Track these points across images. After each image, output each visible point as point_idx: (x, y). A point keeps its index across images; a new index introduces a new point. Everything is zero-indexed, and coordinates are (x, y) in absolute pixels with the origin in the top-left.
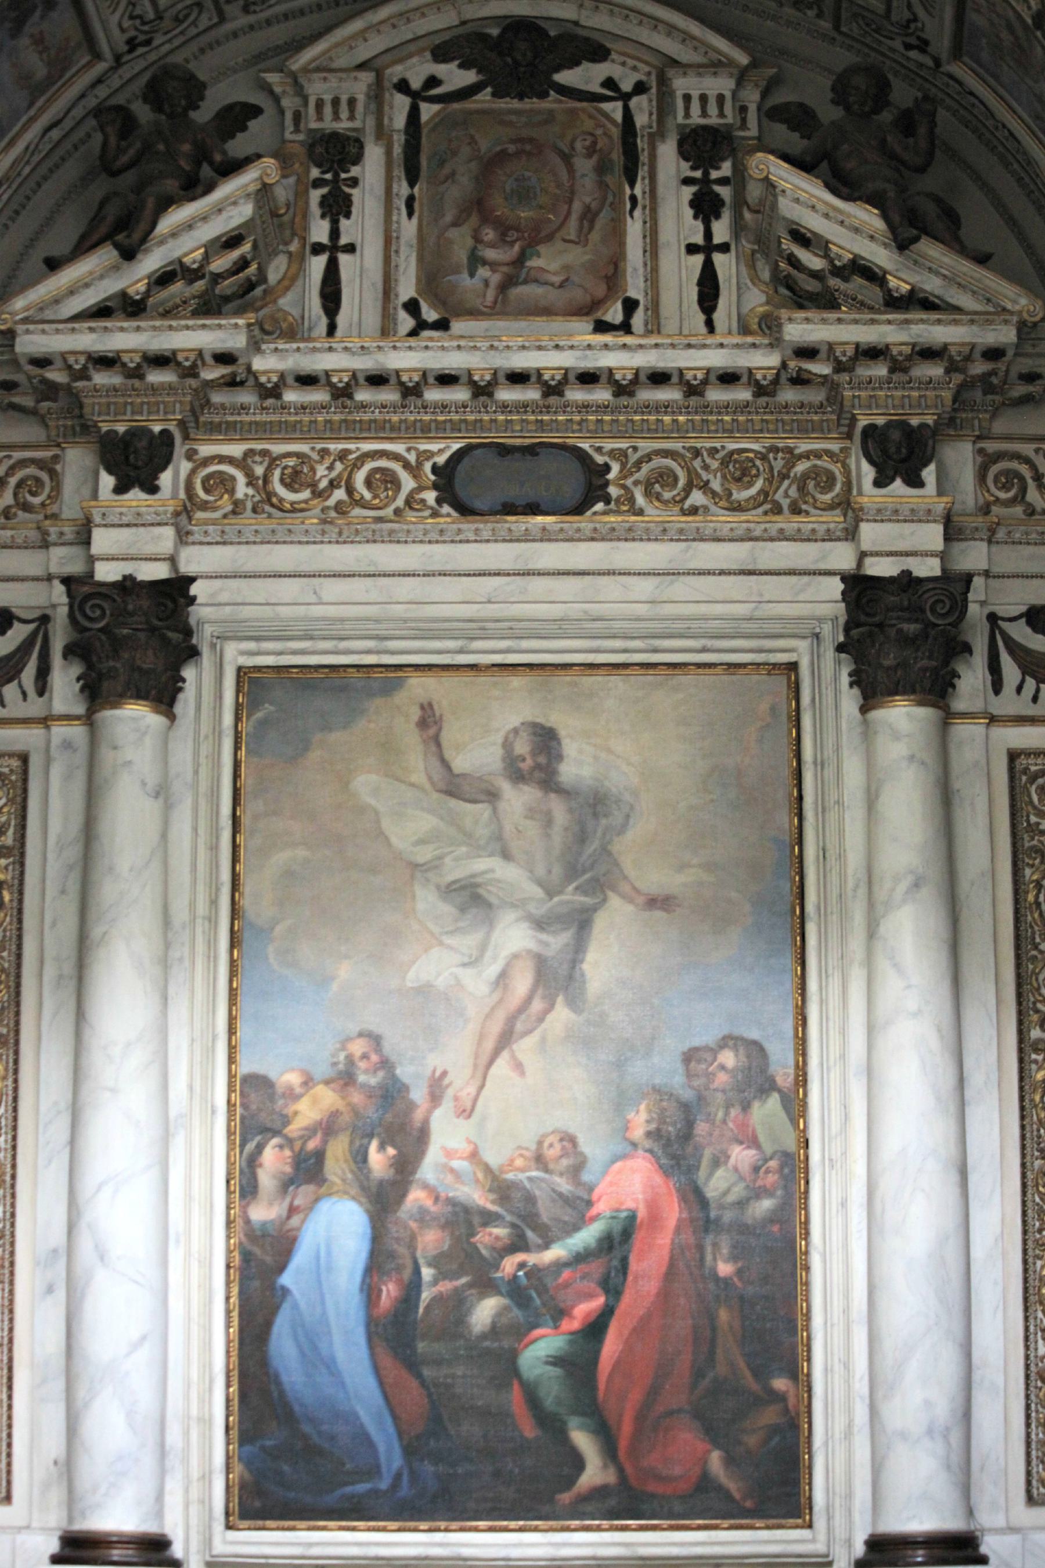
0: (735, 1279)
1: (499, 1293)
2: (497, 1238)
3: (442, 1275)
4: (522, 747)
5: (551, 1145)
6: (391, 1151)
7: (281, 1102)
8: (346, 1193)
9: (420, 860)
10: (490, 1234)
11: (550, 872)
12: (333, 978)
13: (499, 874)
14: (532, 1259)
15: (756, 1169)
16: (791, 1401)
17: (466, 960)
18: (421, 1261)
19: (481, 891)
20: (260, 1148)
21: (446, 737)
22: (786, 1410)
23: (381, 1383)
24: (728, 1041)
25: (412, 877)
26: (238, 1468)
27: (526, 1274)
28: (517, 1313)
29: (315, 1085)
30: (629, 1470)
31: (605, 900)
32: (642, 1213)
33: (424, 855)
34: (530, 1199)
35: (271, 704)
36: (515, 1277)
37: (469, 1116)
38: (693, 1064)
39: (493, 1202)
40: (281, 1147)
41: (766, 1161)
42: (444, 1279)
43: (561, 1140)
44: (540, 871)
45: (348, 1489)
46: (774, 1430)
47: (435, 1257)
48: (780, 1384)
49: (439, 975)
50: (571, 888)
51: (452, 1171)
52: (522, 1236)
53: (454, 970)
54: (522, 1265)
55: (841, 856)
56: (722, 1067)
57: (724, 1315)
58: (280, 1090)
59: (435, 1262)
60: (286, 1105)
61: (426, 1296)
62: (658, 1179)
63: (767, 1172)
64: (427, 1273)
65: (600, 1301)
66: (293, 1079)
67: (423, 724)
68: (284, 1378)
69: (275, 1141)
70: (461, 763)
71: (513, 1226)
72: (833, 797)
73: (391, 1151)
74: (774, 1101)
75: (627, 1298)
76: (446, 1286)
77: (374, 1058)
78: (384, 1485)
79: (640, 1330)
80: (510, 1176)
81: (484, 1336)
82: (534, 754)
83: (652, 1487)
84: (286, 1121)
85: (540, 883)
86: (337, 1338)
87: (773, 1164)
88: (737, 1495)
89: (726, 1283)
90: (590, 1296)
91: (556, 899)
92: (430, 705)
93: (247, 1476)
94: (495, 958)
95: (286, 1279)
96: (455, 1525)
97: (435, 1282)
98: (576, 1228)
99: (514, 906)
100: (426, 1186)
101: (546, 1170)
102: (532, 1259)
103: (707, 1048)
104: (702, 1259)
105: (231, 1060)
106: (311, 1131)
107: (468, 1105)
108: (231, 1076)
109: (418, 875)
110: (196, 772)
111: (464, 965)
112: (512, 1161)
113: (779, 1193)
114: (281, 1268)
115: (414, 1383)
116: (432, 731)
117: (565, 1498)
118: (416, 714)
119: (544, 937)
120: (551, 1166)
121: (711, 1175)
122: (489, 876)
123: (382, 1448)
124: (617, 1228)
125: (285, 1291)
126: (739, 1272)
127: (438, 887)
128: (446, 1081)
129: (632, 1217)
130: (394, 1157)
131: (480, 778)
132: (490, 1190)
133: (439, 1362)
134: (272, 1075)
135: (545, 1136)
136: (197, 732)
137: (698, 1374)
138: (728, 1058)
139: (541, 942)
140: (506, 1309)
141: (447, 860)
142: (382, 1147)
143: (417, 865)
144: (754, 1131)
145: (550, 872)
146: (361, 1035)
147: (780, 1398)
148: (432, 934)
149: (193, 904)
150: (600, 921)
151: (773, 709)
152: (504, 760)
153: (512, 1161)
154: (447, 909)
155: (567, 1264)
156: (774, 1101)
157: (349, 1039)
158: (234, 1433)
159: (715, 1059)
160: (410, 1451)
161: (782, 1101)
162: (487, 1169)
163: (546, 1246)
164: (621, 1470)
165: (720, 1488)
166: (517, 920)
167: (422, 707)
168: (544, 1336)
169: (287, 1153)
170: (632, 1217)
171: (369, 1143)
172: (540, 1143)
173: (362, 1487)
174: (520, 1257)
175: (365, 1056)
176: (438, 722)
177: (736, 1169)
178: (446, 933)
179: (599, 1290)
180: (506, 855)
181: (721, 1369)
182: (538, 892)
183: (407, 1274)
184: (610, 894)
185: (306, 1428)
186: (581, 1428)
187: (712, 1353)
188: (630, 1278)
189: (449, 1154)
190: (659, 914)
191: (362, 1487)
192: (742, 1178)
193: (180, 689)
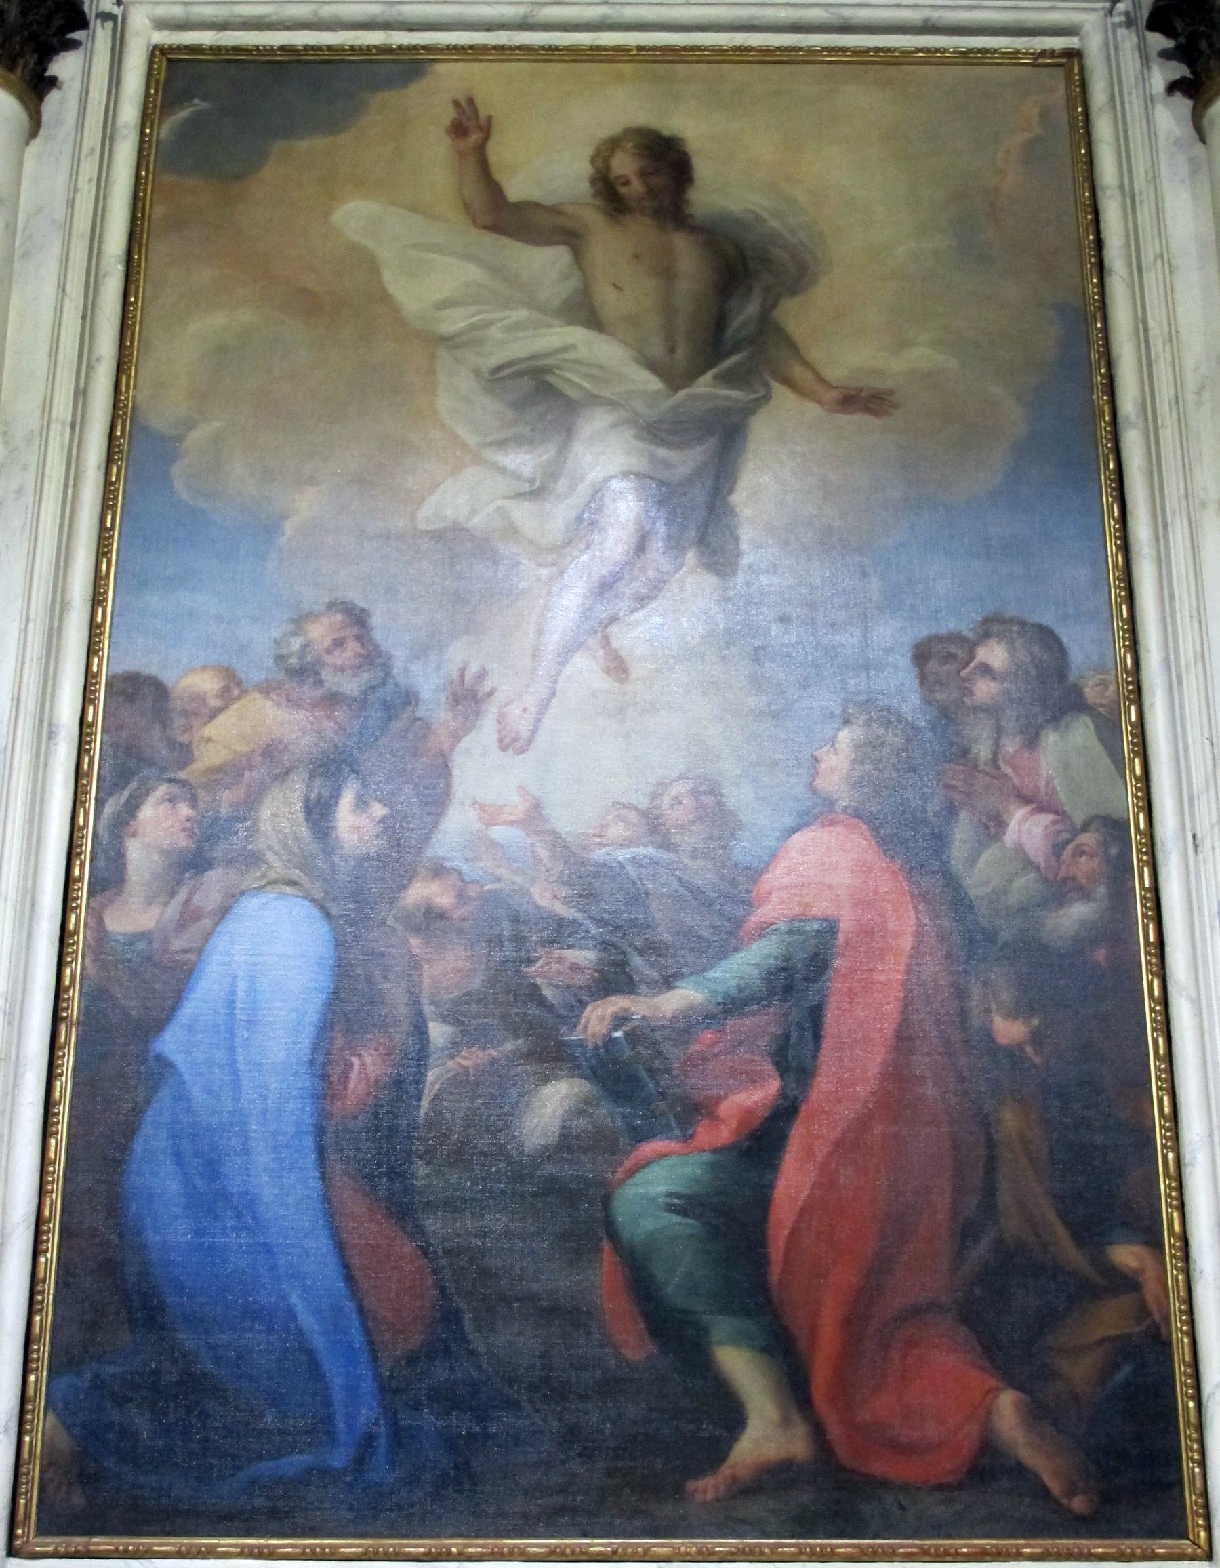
0: (1029, 1050)
1: (576, 1070)
2: (575, 967)
3: (467, 1037)
4: (624, 165)
5: (677, 801)
6: (379, 810)
7: (179, 722)
8: (292, 883)
9: (446, 328)
10: (560, 960)
11: (672, 350)
12: (284, 517)
13: (582, 353)
14: (640, 1007)
15: (1057, 849)
16: (1151, 1289)
17: (526, 487)
18: (428, 1009)
19: (550, 378)
20: (132, 808)
21: (497, 153)
22: (1143, 1310)
23: (340, 1247)
24: (991, 626)
25: (433, 357)
26: (41, 1422)
27: (627, 1034)
28: (608, 1114)
29: (244, 692)
30: (835, 1431)
31: (767, 397)
32: (846, 925)
33: (455, 322)
34: (637, 897)
35: (204, 98)
36: (610, 1042)
37: (522, 751)
38: (932, 665)
39: (566, 901)
40: (172, 800)
41: (1075, 833)
42: (470, 1045)
43: (695, 793)
44: (656, 348)
45: (264, 1468)
46: (1122, 1349)
47: (456, 1003)
48: (1126, 1255)
49: (474, 512)
50: (708, 377)
51: (493, 843)
52: (621, 965)
53: (499, 503)
54: (621, 1019)
55: (1172, 337)
56: (985, 669)
57: (1009, 1119)
58: (177, 704)
59: (452, 1016)
60: (188, 729)
61: (433, 1076)
62: (879, 861)
63: (1079, 852)
64: (438, 1032)
65: (773, 1086)
66: (207, 684)
67: (458, 130)
68: (152, 1238)
69: (162, 790)
70: (516, 189)
71: (605, 946)
72: (1149, 251)
73: (379, 810)
74: (1081, 732)
75: (823, 1084)
76: (472, 1059)
77: (352, 646)
78: (339, 1458)
79: (847, 1146)
80: (599, 855)
81: (546, 1154)
82: (643, 174)
83: (879, 1467)
84: (184, 754)
85: (653, 366)
86: (263, 1158)
87: (1088, 839)
88: (1054, 1486)
89: (1013, 1054)
90: (754, 1078)
91: (682, 393)
92: (471, 101)
93: (64, 1442)
94: (572, 489)
95: (170, 1043)
96: (476, 1546)
97: (454, 1046)
98: (724, 954)
99: (611, 404)
100: (438, 871)
101: (667, 846)
102: (640, 1007)
103: (955, 638)
104: (964, 1014)
105: (92, 649)
106: (229, 772)
107: (524, 733)
108: (90, 678)
109: (442, 353)
110: (71, 203)
111: (520, 495)
112: (604, 826)
113: (1102, 890)
114: (160, 1025)
115: (407, 1247)
116: (474, 138)
117: (707, 1487)
118: (450, 114)
119: (662, 452)
120: (676, 839)
121: (973, 859)
122: (567, 356)
123: (337, 1380)
124: (800, 956)
125: (165, 1064)
126: (1036, 1037)
127: (477, 373)
128: (487, 685)
129: (830, 929)
130: (383, 820)
131: (555, 210)
132: (561, 881)
133: (454, 1205)
134: (167, 677)
135: (663, 785)
136: (78, 144)
137: (967, 1233)
138: (995, 654)
139: (653, 458)
140: (587, 1101)
141: (495, 332)
142: (361, 803)
143: (444, 340)
144: (1049, 781)
145: (672, 350)
146: (331, 606)
147: (1128, 1283)
148: (465, 446)
149: (47, 405)
150: (761, 429)
151: (1044, 116)
152: (593, 181)
153: (604, 826)
154: (489, 408)
155: (709, 1017)
156: (1081, 732)
157: (311, 616)
158: (43, 1351)
159: (972, 657)
160: (388, 1390)
161: (1098, 729)
162: (556, 841)
163: (668, 982)
164: (818, 1431)
165: (1020, 1471)
166: (614, 426)
167: (457, 104)
168: (663, 1156)
169: (185, 810)
170: (830, 929)
171: (335, 796)
172: (654, 796)
173: (294, 1463)
174: (616, 1004)
175: (339, 643)
176: (487, 131)
177: (1019, 848)
178: (491, 444)
179: (768, 1067)
180: (594, 320)
181: (1011, 1225)
182: (654, 383)
183: (400, 1035)
184: (777, 388)
185: (187, 1339)
186: (737, 1340)
187: (990, 1191)
188: (827, 1043)
189: (490, 814)
190: (859, 418)
191: (294, 1463)
192: (1029, 864)
193: (53, 82)
